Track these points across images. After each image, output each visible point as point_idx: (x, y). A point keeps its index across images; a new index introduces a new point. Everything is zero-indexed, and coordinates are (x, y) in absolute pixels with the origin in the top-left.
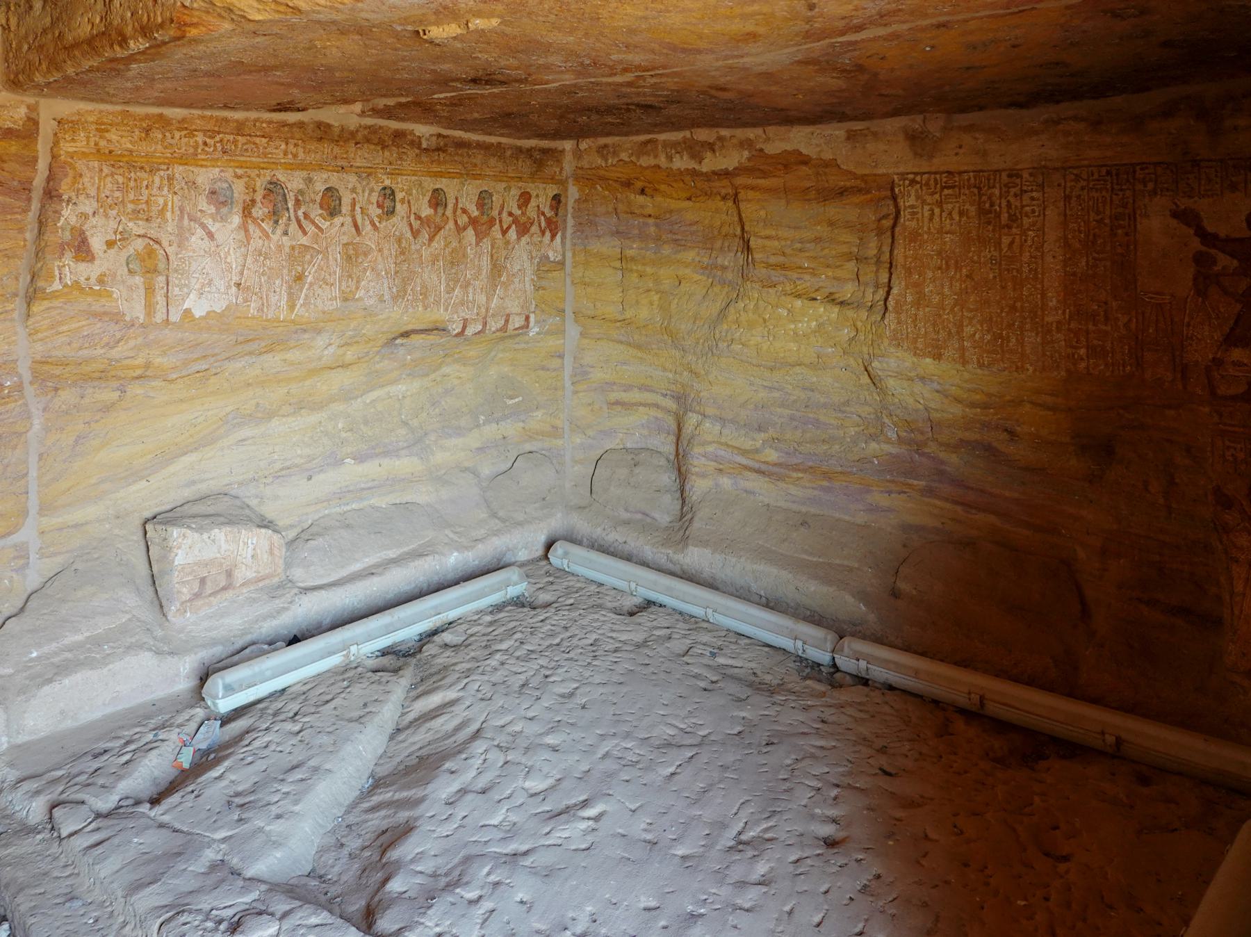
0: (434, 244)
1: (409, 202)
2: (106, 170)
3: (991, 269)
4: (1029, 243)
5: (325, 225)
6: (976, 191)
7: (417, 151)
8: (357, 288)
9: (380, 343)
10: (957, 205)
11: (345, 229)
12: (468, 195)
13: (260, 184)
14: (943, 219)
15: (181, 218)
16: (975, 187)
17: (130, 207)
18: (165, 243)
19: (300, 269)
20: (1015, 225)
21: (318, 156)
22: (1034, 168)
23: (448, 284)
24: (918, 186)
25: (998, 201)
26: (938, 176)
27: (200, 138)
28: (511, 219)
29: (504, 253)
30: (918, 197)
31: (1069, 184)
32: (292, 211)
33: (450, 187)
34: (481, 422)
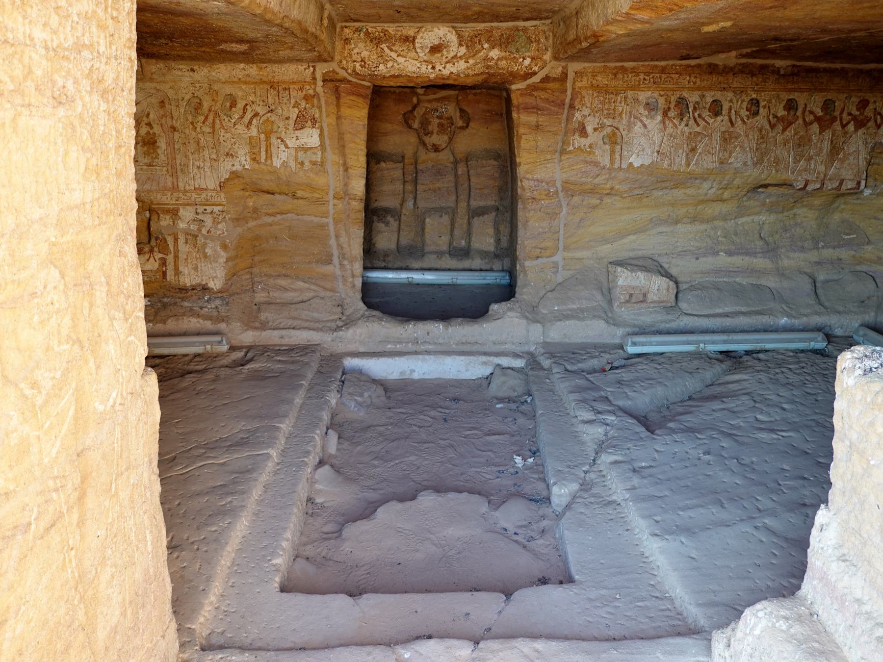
0: (787, 133)
1: (769, 107)
2: (595, 94)
5: (711, 121)
7: (777, 76)
8: (730, 157)
9: (746, 189)
11: (724, 123)
12: (814, 102)
13: (673, 99)
15: (630, 117)
17: (606, 112)
18: (621, 130)
19: (694, 145)
21: (709, 83)
23: (795, 158)
27: (642, 76)
28: (850, 117)
29: (842, 140)
32: (691, 113)
33: (801, 98)
34: (820, 246)
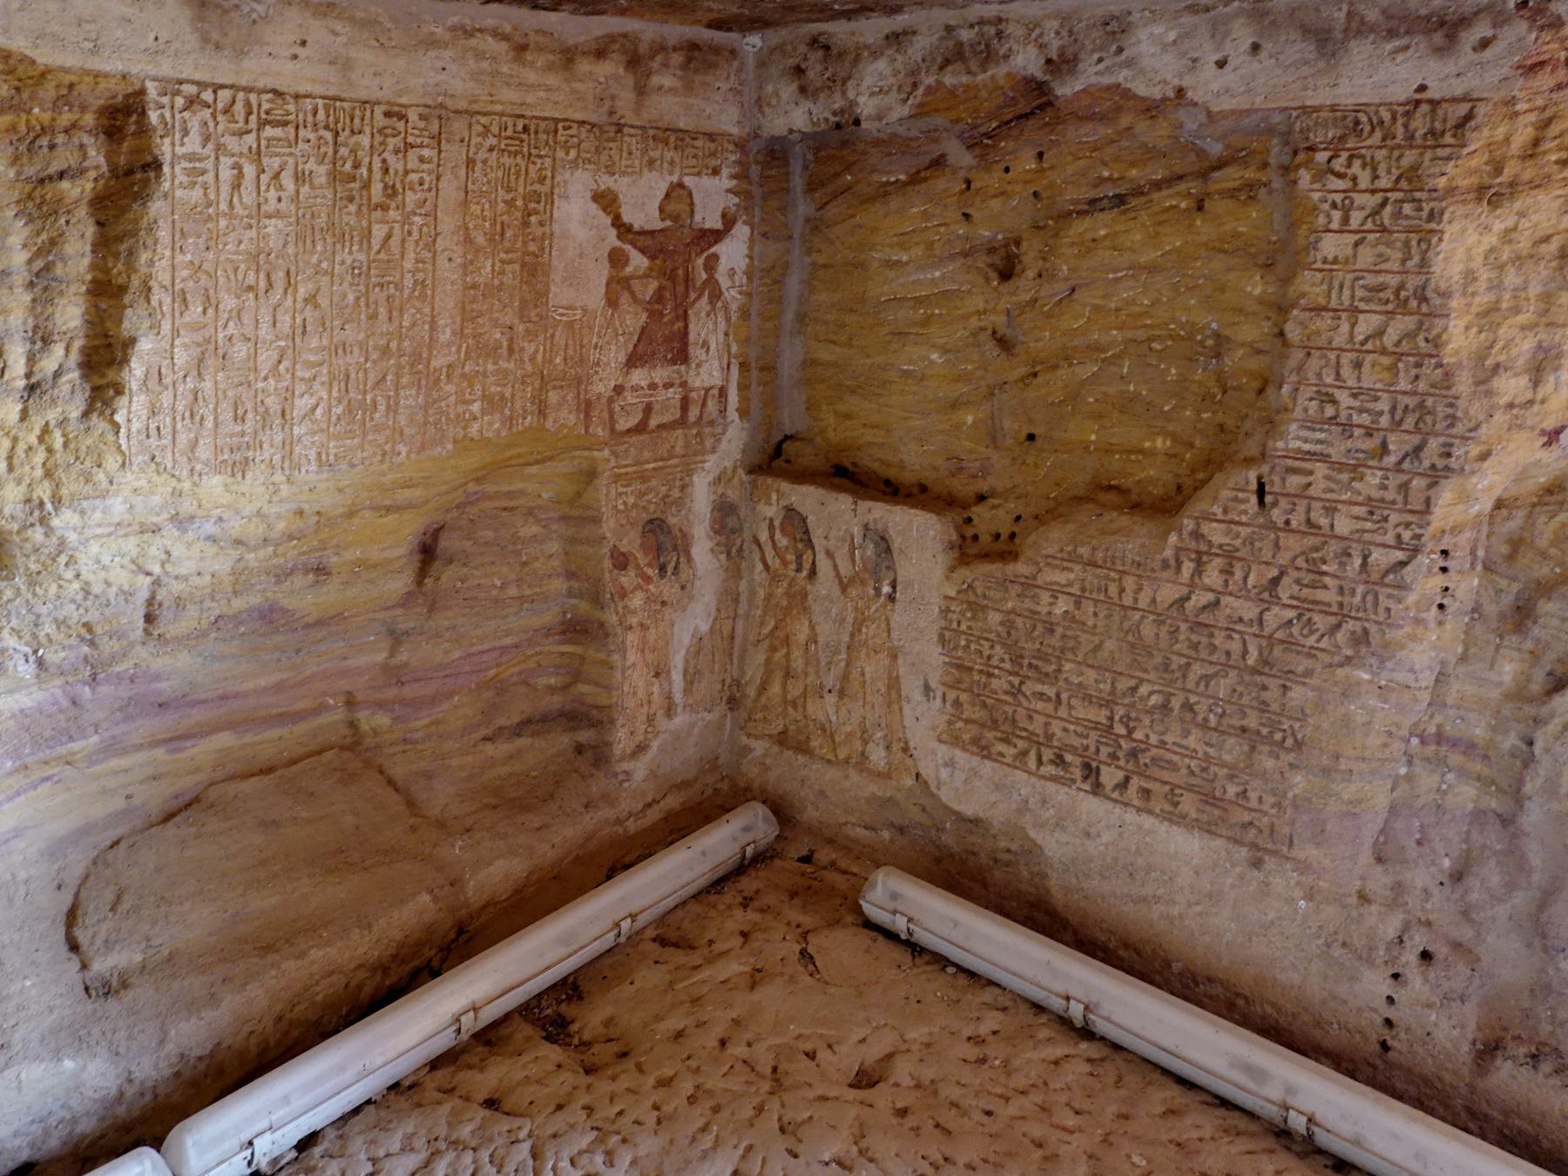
3: (352, 284)
4: (416, 234)
6: (328, 136)
10: (291, 161)
14: (263, 188)
16: (327, 127)
20: (393, 205)
22: (426, 106)
24: (207, 113)
25: (367, 160)
26: (253, 97)
30: (206, 139)
31: (473, 142)
